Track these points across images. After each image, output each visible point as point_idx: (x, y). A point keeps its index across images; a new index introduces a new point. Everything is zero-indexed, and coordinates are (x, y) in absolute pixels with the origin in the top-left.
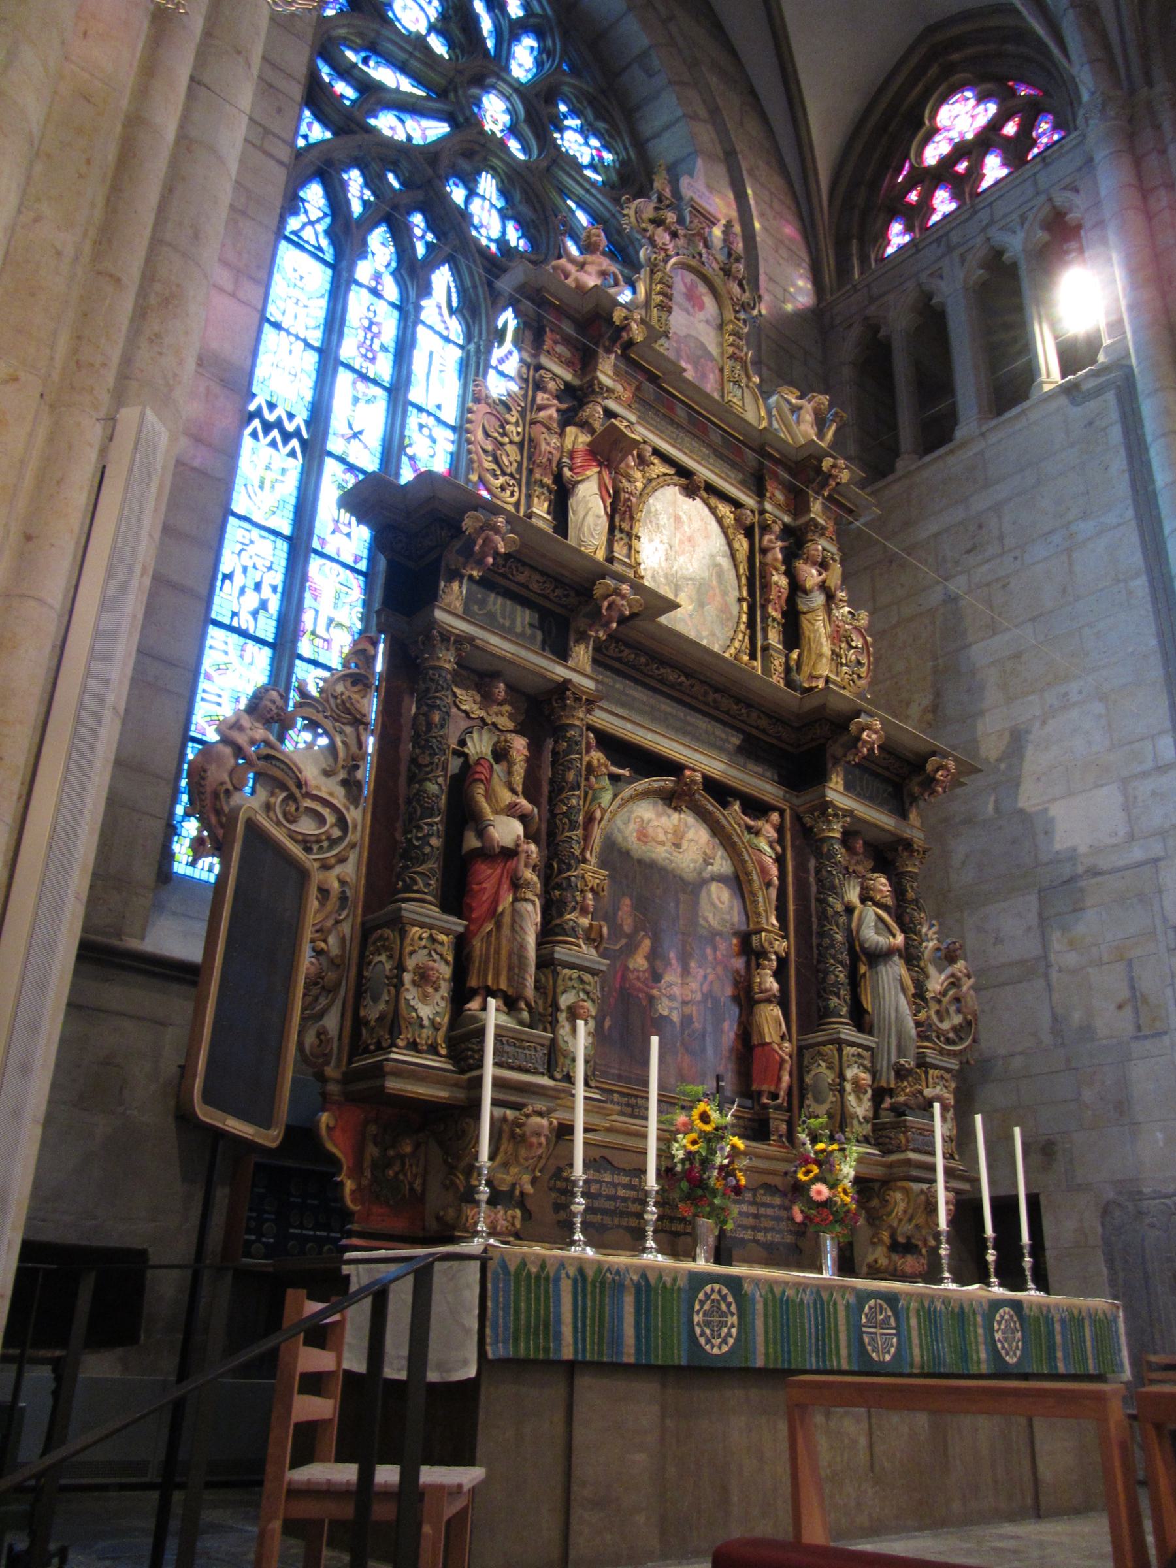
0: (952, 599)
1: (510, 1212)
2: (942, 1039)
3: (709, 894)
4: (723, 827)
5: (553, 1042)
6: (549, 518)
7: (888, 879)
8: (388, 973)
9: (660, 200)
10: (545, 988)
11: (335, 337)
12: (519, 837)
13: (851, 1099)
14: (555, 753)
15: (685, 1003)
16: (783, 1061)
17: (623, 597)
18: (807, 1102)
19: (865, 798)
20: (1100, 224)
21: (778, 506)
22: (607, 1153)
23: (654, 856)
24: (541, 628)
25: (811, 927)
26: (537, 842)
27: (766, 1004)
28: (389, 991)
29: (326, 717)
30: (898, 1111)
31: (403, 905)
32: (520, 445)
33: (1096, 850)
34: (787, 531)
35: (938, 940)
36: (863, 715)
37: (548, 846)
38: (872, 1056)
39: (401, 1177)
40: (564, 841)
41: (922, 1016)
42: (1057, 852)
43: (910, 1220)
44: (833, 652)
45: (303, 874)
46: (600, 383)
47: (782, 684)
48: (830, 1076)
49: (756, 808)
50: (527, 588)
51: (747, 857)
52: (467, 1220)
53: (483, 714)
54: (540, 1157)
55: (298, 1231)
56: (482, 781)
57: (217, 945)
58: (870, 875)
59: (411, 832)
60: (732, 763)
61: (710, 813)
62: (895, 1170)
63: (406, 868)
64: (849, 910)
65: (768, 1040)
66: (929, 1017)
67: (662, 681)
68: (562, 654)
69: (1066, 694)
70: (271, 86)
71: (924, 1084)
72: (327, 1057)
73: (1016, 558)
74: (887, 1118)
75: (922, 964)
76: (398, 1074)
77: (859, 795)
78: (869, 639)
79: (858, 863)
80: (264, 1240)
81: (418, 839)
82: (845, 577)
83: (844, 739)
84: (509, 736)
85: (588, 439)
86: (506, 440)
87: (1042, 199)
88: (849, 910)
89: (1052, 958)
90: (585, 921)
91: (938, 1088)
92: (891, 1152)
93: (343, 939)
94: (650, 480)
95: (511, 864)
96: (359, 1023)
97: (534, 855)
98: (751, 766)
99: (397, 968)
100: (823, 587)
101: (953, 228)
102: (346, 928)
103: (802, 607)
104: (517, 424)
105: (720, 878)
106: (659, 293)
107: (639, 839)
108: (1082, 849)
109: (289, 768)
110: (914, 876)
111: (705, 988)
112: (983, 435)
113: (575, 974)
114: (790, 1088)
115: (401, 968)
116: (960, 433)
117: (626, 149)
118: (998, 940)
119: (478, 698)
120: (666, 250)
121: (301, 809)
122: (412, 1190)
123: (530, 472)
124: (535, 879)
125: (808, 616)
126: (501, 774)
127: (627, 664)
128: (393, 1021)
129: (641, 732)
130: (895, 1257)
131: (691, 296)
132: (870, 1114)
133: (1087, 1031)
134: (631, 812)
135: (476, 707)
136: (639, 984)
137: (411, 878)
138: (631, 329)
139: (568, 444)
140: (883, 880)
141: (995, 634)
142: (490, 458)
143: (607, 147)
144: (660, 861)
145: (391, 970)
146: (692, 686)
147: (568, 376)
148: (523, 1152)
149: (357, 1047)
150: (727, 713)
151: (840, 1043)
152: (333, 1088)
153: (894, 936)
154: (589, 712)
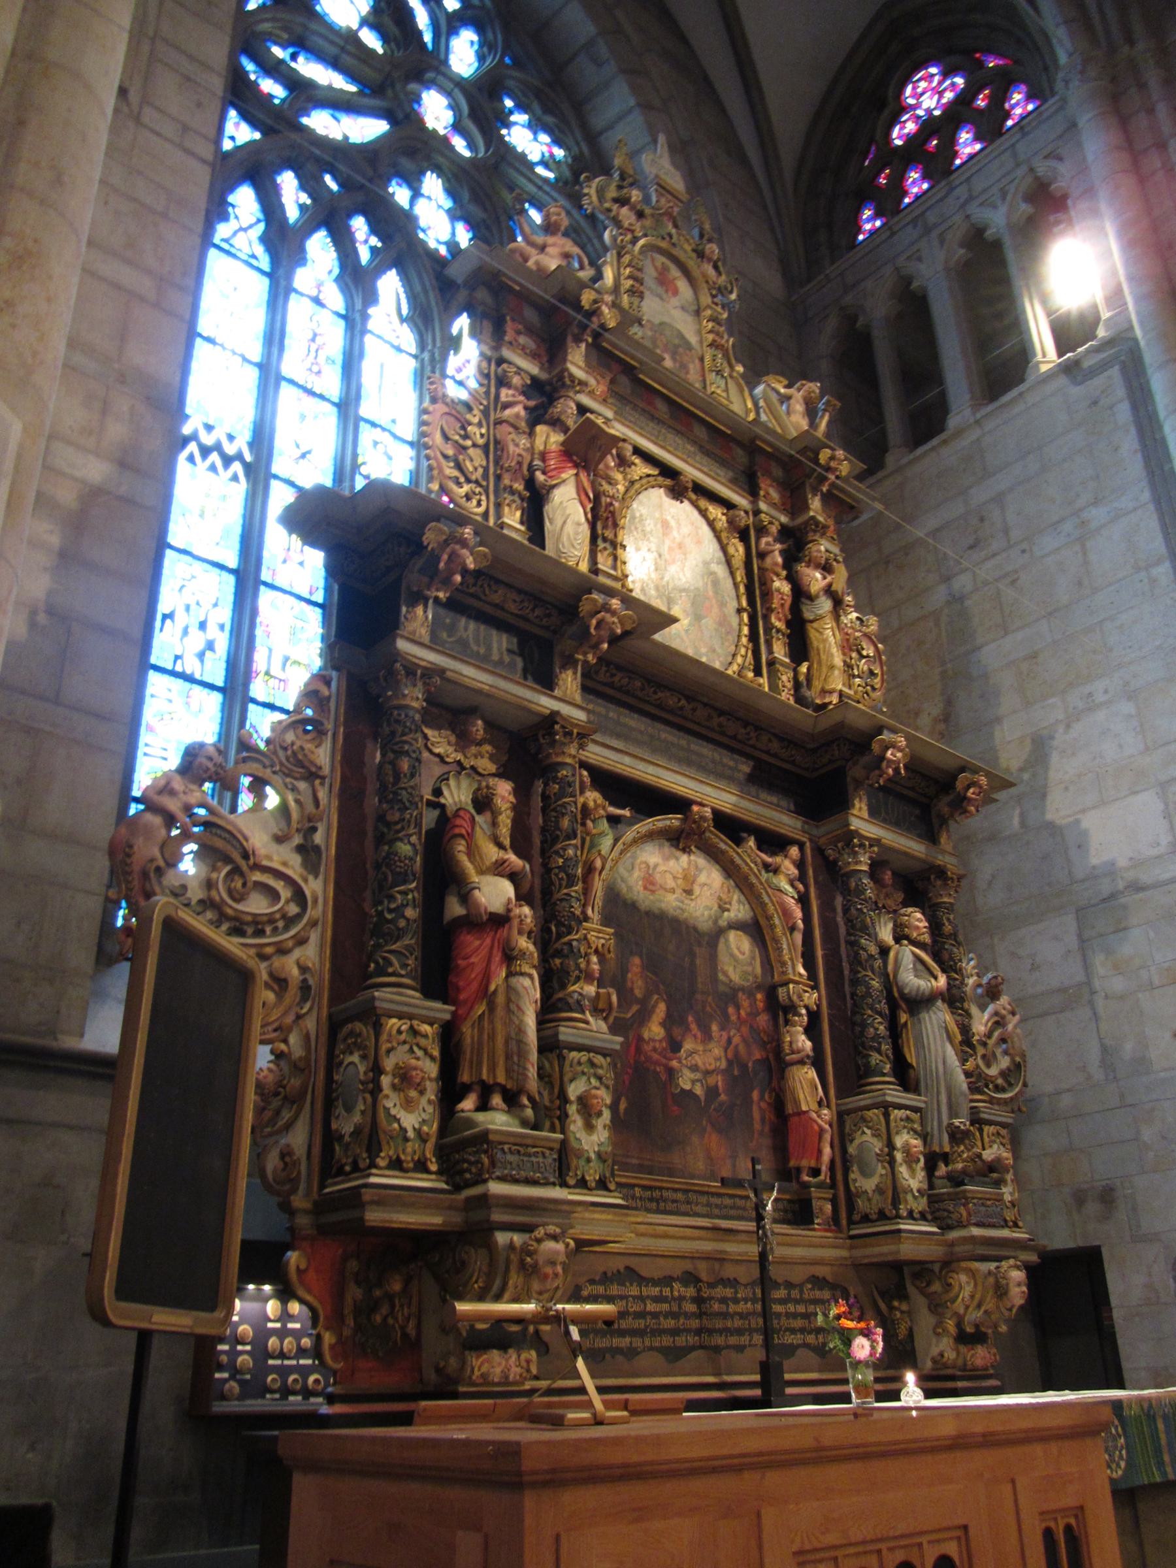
0: (957, 599)
1: (524, 1356)
2: (991, 1086)
4: (738, 867)
5: (564, 1143)
6: (523, 528)
7: (923, 914)
8: (362, 1077)
9: (623, 177)
10: (550, 1076)
11: (275, 351)
12: (509, 900)
13: (903, 1170)
14: (545, 797)
15: (707, 1073)
16: (822, 1130)
17: (614, 613)
18: (852, 1176)
19: (890, 823)
20: (1090, 192)
21: (773, 505)
22: (633, 1262)
23: (663, 905)
24: (521, 655)
25: (842, 972)
26: (531, 904)
27: (799, 1066)
28: (364, 1099)
29: (274, 773)
30: (956, 1180)
31: (376, 994)
32: (485, 448)
33: (1137, 863)
34: (785, 533)
35: (978, 975)
36: (885, 732)
37: (544, 906)
38: (921, 1117)
39: (390, 1321)
40: (561, 900)
41: (969, 1065)
42: (1094, 867)
43: (979, 1306)
44: (845, 662)
45: (246, 977)
46: (571, 376)
47: (792, 701)
48: (877, 1145)
49: (773, 842)
50: (503, 609)
51: (766, 900)
52: (472, 1371)
53: (459, 757)
54: (557, 1288)
55: (278, 1362)
56: (462, 836)
57: (129, 1087)
58: (903, 911)
59: (381, 903)
60: (744, 793)
61: (723, 852)
62: (957, 1249)
63: (377, 946)
64: (884, 951)
65: (804, 1108)
66: (978, 1066)
68: (547, 683)
69: (1090, 694)
70: (188, 79)
71: (979, 1143)
72: (294, 1182)
73: (1023, 551)
74: (944, 1190)
75: (966, 1005)
76: (379, 1203)
77: (884, 821)
78: (880, 646)
79: (887, 896)
80: (238, 1377)
81: (390, 911)
82: (850, 581)
83: (865, 759)
84: (492, 781)
85: (561, 438)
86: (469, 443)
87: (1023, 169)
88: (884, 951)
89: (1097, 984)
90: (591, 990)
91: (995, 1146)
92: (950, 1228)
93: (307, 1037)
94: (632, 483)
95: (501, 933)
96: (330, 1138)
97: (529, 920)
98: (764, 795)
99: (372, 1070)
100: (829, 591)
101: (928, 209)
102: (310, 1024)
103: (808, 615)
104: (480, 425)
106: (629, 277)
107: (645, 888)
108: (1122, 862)
109: (233, 837)
110: (950, 908)
111: (730, 1054)
112: (977, 422)
113: (583, 1056)
114: (832, 1161)
115: (377, 1070)
116: (953, 422)
117: (577, 144)
118: (1034, 968)
119: (453, 739)
120: (633, 231)
121: (250, 884)
122: (405, 1335)
123: (498, 478)
124: (532, 947)
125: (815, 625)
126: (485, 826)
127: (620, 689)
128: (371, 1136)
129: (641, 766)
130: (963, 1349)
131: (663, 280)
132: (926, 1187)
133: (1141, 1064)
134: (634, 857)
135: (451, 749)
136: (656, 1056)
137: (384, 958)
138: (602, 313)
139: (539, 444)
140: (919, 915)
141: (1006, 634)
142: (452, 464)
143: (557, 141)
144: (671, 911)
145: (365, 1073)
146: (694, 710)
147: (534, 370)
148: (536, 1286)
149: (329, 1168)
150: (734, 737)
151: (886, 1108)
152: (303, 1221)
153: (936, 978)
154: (582, 747)
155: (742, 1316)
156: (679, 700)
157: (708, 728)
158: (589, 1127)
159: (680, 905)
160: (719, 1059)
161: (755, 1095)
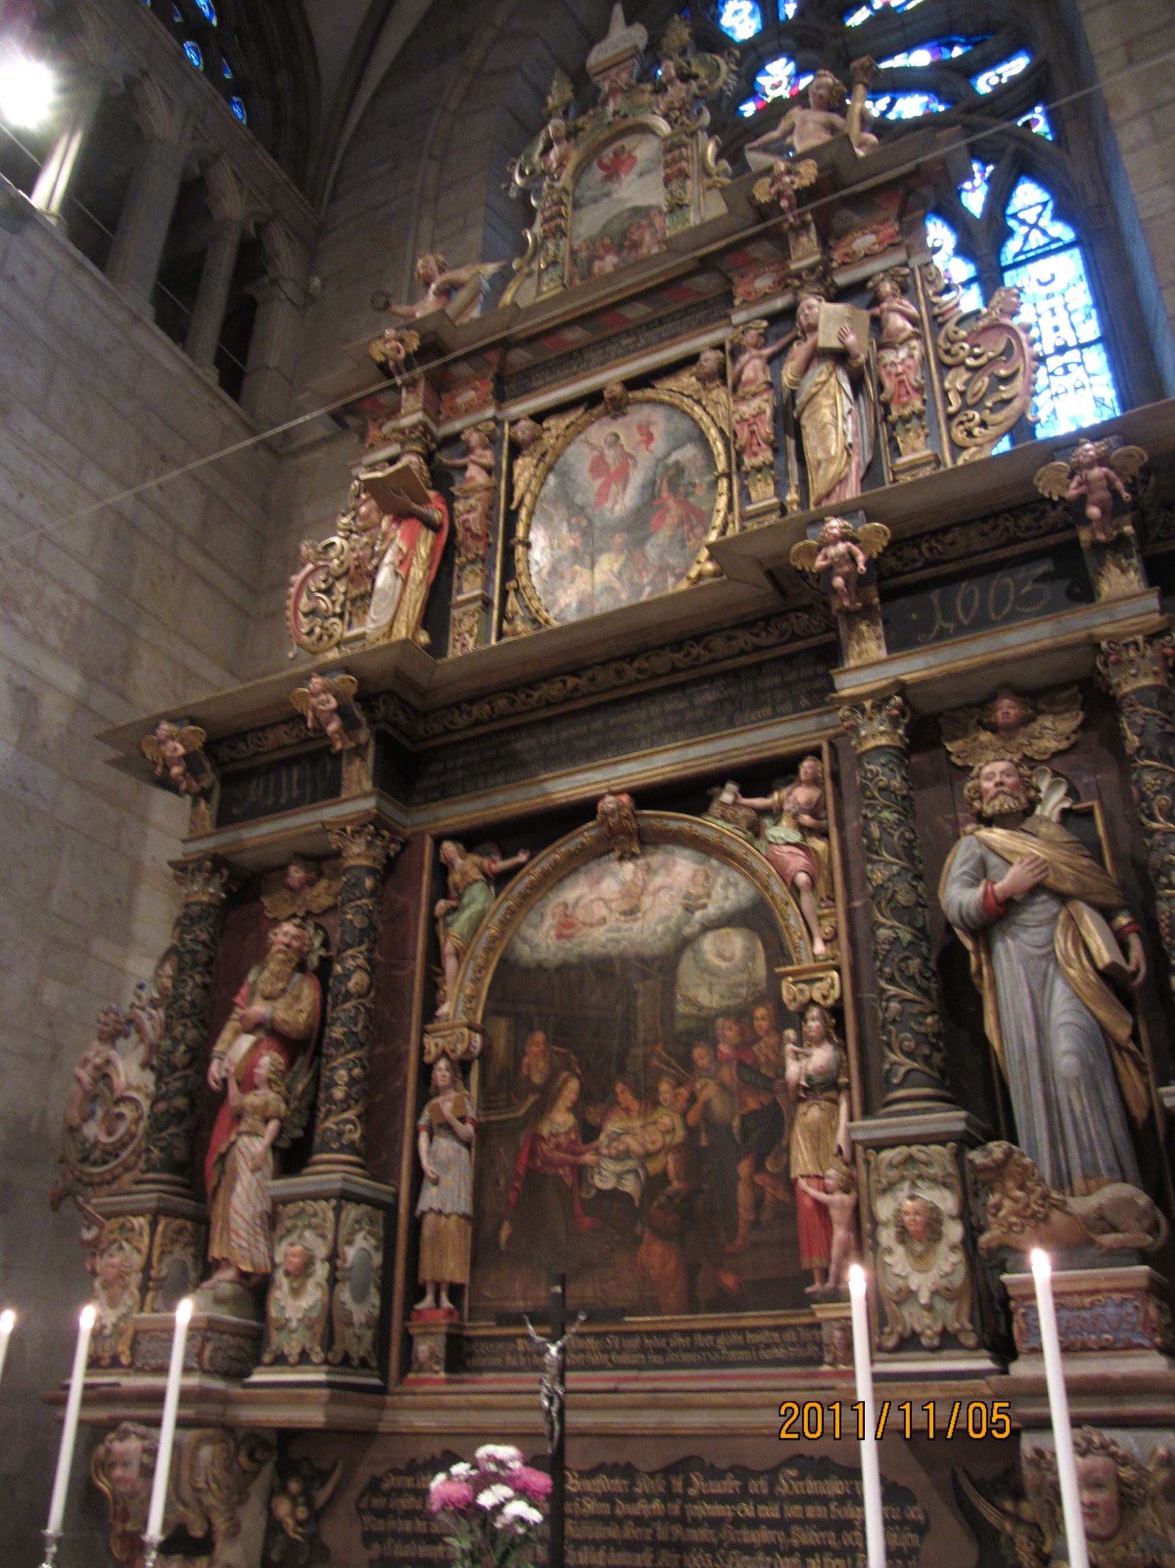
3: (698, 959)
15: (649, 1155)
16: (822, 1209)
23: (586, 949)
50: (286, 746)
67: (549, 704)
105: (728, 920)
107: (560, 936)
111: (692, 1117)
127: (491, 720)
136: (559, 1155)
146: (593, 679)
150: (675, 670)
155: (639, 1521)
156: (564, 682)
157: (631, 684)
158: (296, 1292)
159: (615, 935)
160: (673, 1130)
161: (744, 1168)
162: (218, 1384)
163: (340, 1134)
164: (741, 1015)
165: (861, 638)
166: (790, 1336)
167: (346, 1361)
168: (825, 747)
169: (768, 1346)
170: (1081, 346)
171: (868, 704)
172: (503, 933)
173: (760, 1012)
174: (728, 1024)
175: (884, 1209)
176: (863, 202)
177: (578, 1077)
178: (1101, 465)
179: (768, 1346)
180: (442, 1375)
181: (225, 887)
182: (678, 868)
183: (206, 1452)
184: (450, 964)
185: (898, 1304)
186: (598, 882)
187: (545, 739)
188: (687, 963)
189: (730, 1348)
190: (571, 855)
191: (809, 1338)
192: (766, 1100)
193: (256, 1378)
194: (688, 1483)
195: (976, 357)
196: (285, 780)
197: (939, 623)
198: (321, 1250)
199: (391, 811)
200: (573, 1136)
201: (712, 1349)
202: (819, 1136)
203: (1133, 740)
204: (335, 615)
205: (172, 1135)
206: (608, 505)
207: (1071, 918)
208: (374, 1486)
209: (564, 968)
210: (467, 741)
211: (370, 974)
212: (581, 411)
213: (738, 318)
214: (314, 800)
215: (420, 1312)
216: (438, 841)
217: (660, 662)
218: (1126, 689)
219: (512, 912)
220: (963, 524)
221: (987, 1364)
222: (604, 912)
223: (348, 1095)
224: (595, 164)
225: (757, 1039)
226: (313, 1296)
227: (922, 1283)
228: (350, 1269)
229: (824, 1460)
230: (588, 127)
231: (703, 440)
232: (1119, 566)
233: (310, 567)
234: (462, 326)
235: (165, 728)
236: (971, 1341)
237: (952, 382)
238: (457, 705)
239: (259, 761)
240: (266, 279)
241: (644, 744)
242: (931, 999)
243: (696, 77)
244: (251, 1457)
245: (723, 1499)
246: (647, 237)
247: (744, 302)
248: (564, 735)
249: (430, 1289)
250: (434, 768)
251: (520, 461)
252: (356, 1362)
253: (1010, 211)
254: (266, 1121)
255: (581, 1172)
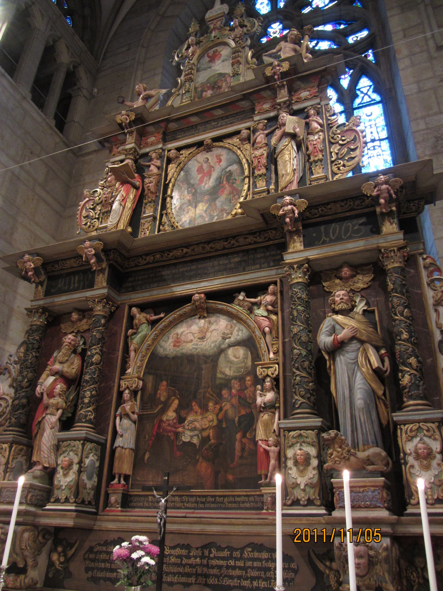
3: (226, 357)
15: (203, 430)
16: (267, 452)
23: (184, 351)
50: (73, 267)
67: (176, 258)
107: (174, 346)
111: (220, 416)
146: (193, 250)
150: (224, 248)
155: (191, 566)
156: (182, 250)
158: (65, 475)
159: (196, 346)
162: (32, 509)
163: (86, 416)
164: (241, 379)
165: (294, 242)
166: (251, 499)
167: (83, 502)
168: (278, 281)
169: (243, 502)
170: (380, 140)
171: (295, 266)
172: (153, 343)
173: (248, 378)
174: (236, 382)
175: (290, 453)
176: (305, 79)
177: (178, 399)
178: (386, 184)
179: (243, 502)
180: (120, 509)
181: (46, 319)
182: (221, 323)
183: (26, 535)
184: (132, 354)
185: (293, 488)
186: (190, 326)
187: (174, 271)
188: (222, 359)
189: (229, 502)
190: (181, 316)
191: (259, 500)
192: (248, 411)
193: (47, 507)
194: (210, 552)
195: (343, 141)
196: (72, 280)
197: (324, 238)
198: (76, 460)
199: (113, 294)
200: (175, 421)
201: (222, 503)
202: (267, 425)
203: (391, 286)
204: (95, 218)
205: (19, 413)
206: (203, 184)
207: (364, 350)
208: (91, 550)
209: (175, 358)
210: (144, 270)
211: (101, 356)
212: (195, 148)
213: (256, 118)
214: (83, 288)
215: (113, 485)
216: (130, 307)
217: (219, 245)
218: (389, 267)
219: (157, 336)
220: (334, 202)
221: (324, 512)
222: (192, 338)
223: (90, 402)
224: (206, 55)
225: (246, 388)
226: (72, 477)
227: (302, 481)
228: (87, 467)
229: (262, 545)
230: (204, 41)
231: (240, 163)
232: (390, 221)
233: (87, 199)
234: (151, 112)
235: (27, 257)
236: (318, 503)
237: (334, 149)
238: (141, 256)
239: (62, 272)
240: (76, 87)
241: (211, 275)
242: (312, 377)
243: (246, 26)
244: (44, 537)
245: (223, 558)
246: (224, 85)
247: (259, 112)
248: (181, 270)
249: (117, 476)
250: (130, 279)
251: (170, 165)
252: (87, 503)
253: (357, 88)
254: (58, 410)
255: (177, 435)
